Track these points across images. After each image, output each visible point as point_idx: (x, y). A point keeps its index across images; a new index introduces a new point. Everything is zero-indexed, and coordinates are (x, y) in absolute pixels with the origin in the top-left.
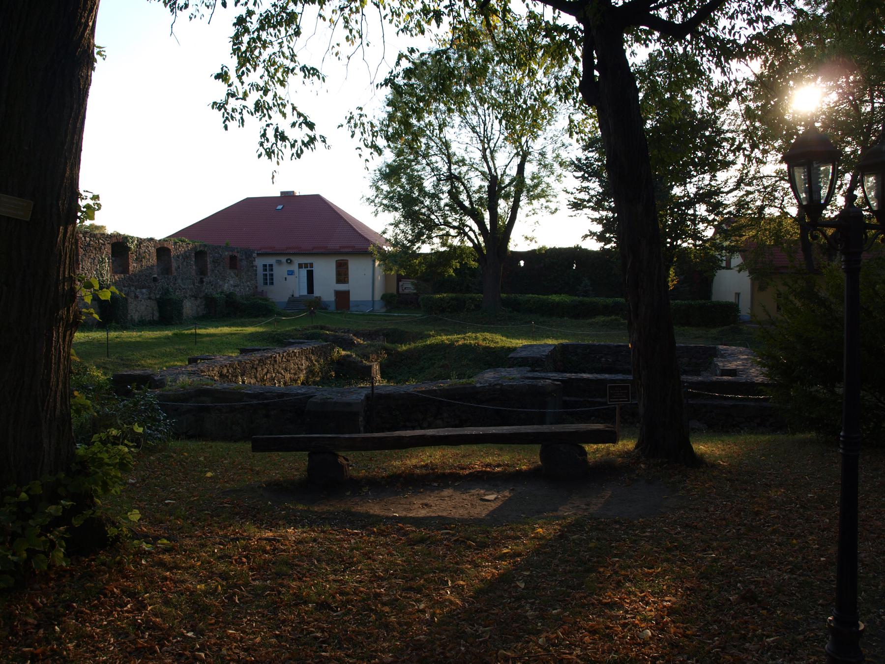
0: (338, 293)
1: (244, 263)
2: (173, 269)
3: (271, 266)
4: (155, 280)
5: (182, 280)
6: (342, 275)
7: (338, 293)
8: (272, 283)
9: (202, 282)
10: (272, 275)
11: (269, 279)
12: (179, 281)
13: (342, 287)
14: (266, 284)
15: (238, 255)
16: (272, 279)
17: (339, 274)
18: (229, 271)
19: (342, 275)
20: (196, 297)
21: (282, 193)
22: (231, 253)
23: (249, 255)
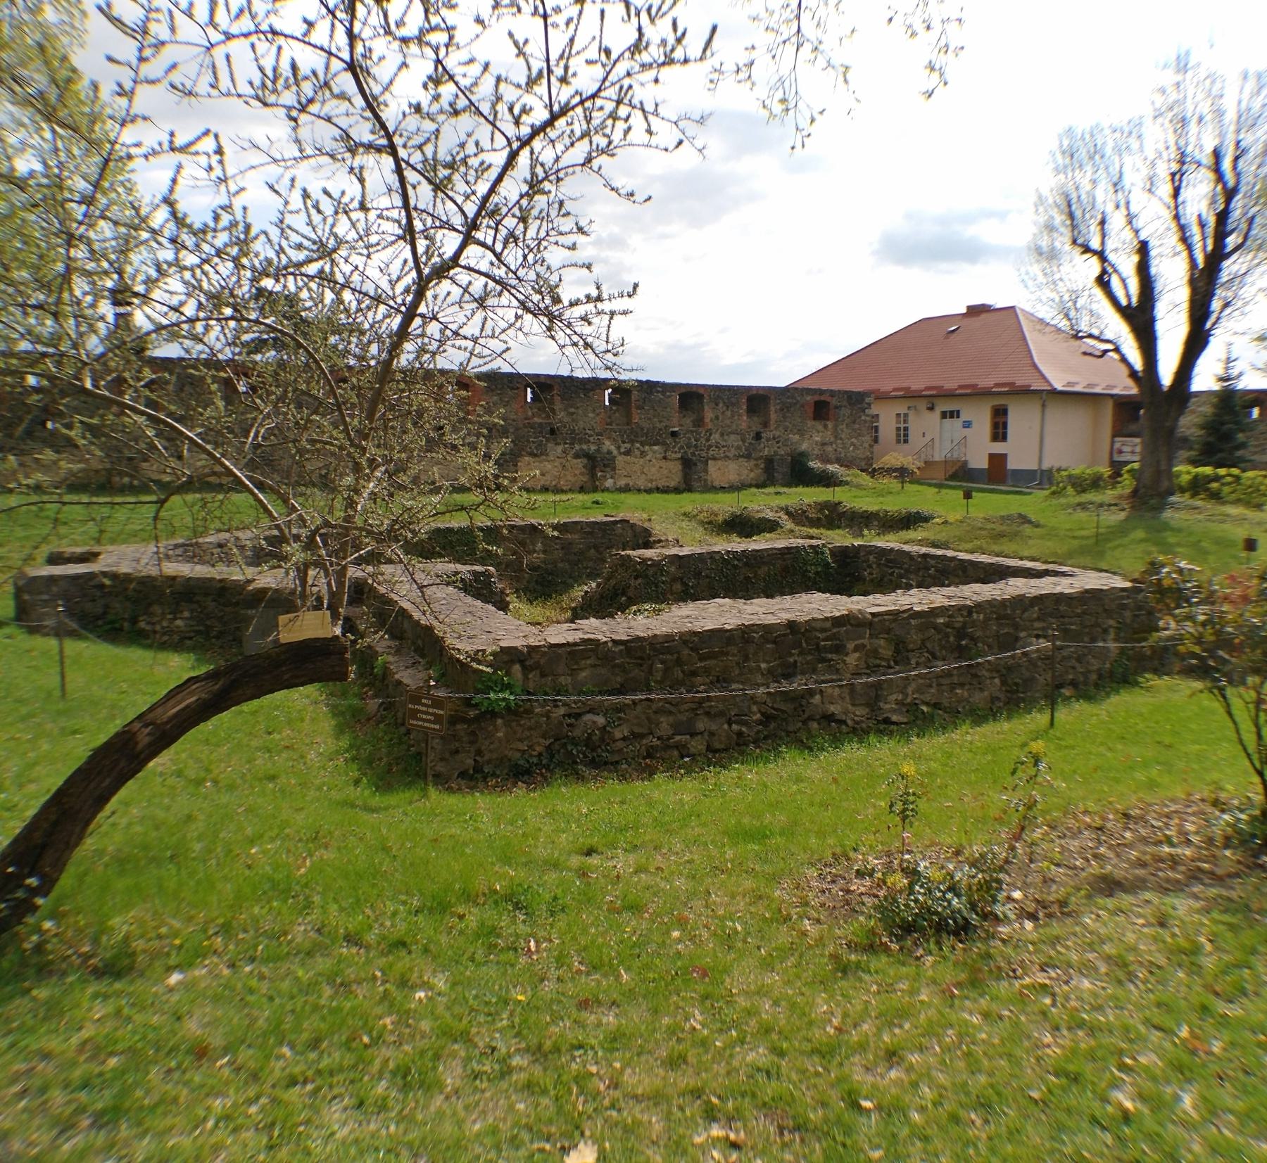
0: (992, 456)
1: (846, 412)
2: (707, 420)
3: (906, 415)
4: (674, 434)
5: (722, 435)
6: (999, 432)
7: (992, 456)
8: (906, 441)
9: (758, 436)
10: (906, 429)
11: (903, 436)
12: (716, 437)
13: (998, 448)
14: (898, 441)
15: (834, 402)
16: (906, 435)
17: (995, 426)
18: (810, 423)
19: (999, 432)
20: (748, 457)
21: (969, 308)
22: (817, 398)
23: (857, 400)
